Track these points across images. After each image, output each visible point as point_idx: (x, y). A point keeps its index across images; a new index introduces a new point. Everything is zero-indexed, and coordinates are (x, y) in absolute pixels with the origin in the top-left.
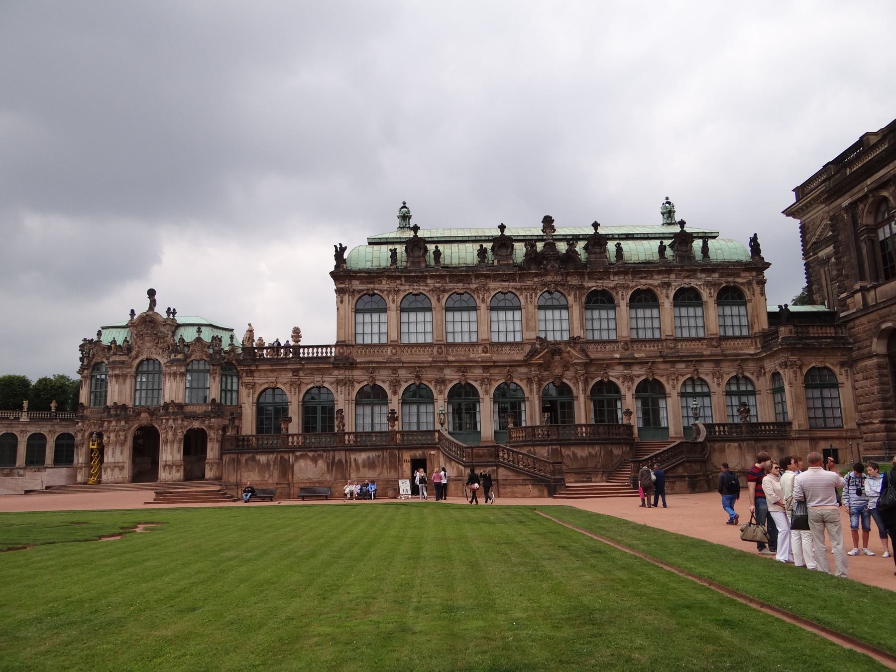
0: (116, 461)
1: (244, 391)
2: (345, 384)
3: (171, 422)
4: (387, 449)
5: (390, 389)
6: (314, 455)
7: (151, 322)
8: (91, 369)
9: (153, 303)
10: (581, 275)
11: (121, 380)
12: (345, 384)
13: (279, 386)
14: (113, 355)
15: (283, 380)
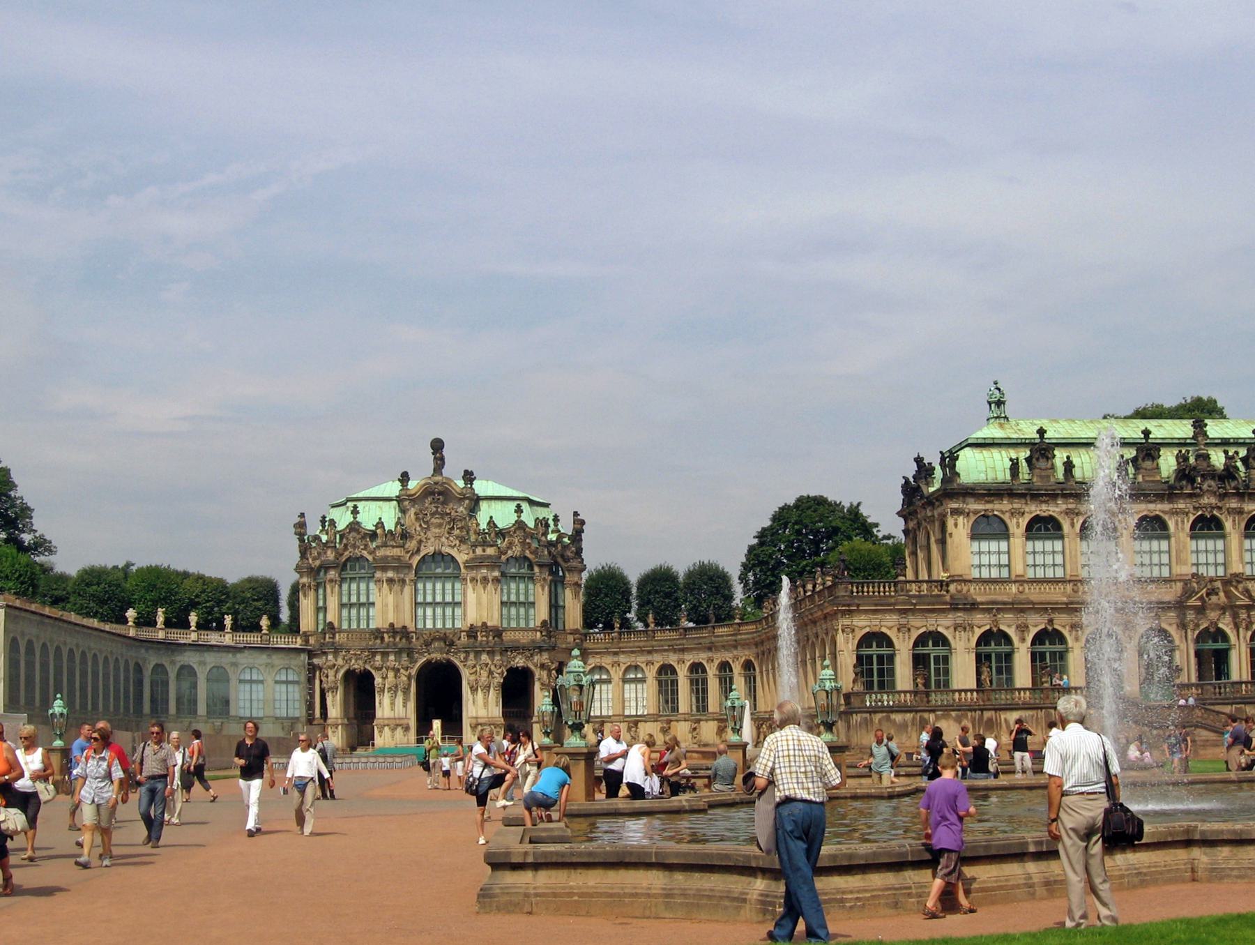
0: (396, 716)
1: (840, 638)
2: (965, 629)
3: (484, 657)
4: (1041, 709)
5: (1016, 635)
6: (957, 716)
7: (440, 493)
8: (340, 568)
9: (440, 463)
10: (1240, 495)
11: (396, 587)
12: (965, 629)
13: (884, 630)
14: (382, 547)
15: (887, 624)
